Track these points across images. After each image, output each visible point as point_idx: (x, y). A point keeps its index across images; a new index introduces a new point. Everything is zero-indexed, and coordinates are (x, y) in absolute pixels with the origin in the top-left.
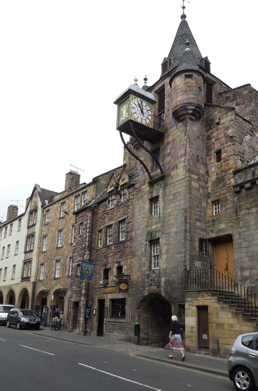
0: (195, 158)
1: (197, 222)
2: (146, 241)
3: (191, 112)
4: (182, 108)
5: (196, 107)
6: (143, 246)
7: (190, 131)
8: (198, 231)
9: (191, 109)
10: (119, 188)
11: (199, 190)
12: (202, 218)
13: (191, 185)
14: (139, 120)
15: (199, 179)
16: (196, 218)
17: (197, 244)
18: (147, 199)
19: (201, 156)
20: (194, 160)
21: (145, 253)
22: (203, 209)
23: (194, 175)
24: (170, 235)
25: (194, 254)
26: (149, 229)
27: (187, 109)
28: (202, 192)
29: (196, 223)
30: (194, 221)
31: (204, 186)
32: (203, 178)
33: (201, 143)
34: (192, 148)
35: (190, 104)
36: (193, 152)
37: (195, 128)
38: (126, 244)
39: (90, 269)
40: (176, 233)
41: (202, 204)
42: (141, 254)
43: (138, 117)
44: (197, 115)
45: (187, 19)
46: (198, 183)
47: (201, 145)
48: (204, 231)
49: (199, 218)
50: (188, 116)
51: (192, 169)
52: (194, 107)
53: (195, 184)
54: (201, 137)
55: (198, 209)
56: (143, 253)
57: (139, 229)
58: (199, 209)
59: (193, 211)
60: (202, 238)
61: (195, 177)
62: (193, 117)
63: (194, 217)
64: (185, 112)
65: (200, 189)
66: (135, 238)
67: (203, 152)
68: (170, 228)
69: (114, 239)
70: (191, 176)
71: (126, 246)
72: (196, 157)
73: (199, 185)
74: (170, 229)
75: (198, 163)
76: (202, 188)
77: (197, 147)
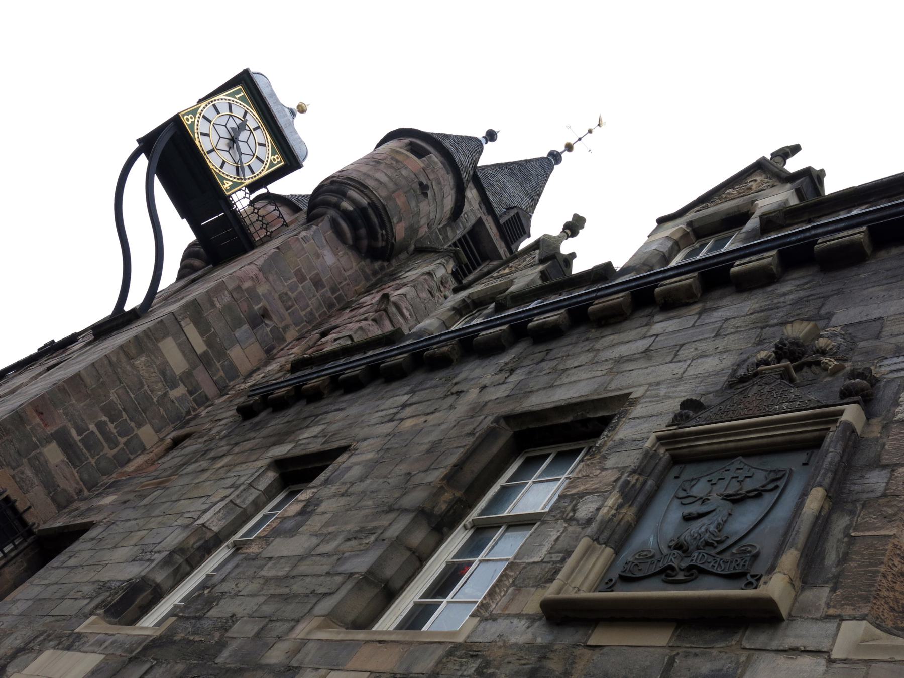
1: (54, 445)
3: (350, 208)
4: (333, 187)
5: (372, 205)
7: (305, 245)
8: (29, 473)
9: (353, 201)
12: (93, 462)
13: (158, 340)
14: (204, 144)
15: (205, 360)
19: (281, 326)
20: (244, 306)
22: (125, 439)
23: (202, 335)
27: (344, 195)
28: (181, 399)
29: (47, 440)
30: (51, 430)
31: (206, 396)
32: (222, 373)
33: (313, 303)
34: (267, 279)
35: (362, 187)
36: (262, 290)
37: (329, 259)
41: (139, 426)
43: (224, 162)
44: (363, 231)
46: (193, 366)
47: (308, 306)
48: (53, 499)
49: (80, 444)
50: (332, 213)
51: (210, 315)
52: (364, 202)
53: (172, 354)
54: (326, 291)
55: (104, 418)
58: (111, 426)
59: (77, 404)
60: (20, 506)
61: (200, 346)
62: (344, 225)
64: (334, 199)
65: (182, 385)
67: (296, 325)
70: (182, 323)
72: (256, 308)
75: (246, 327)
76: (191, 393)
77: (290, 293)
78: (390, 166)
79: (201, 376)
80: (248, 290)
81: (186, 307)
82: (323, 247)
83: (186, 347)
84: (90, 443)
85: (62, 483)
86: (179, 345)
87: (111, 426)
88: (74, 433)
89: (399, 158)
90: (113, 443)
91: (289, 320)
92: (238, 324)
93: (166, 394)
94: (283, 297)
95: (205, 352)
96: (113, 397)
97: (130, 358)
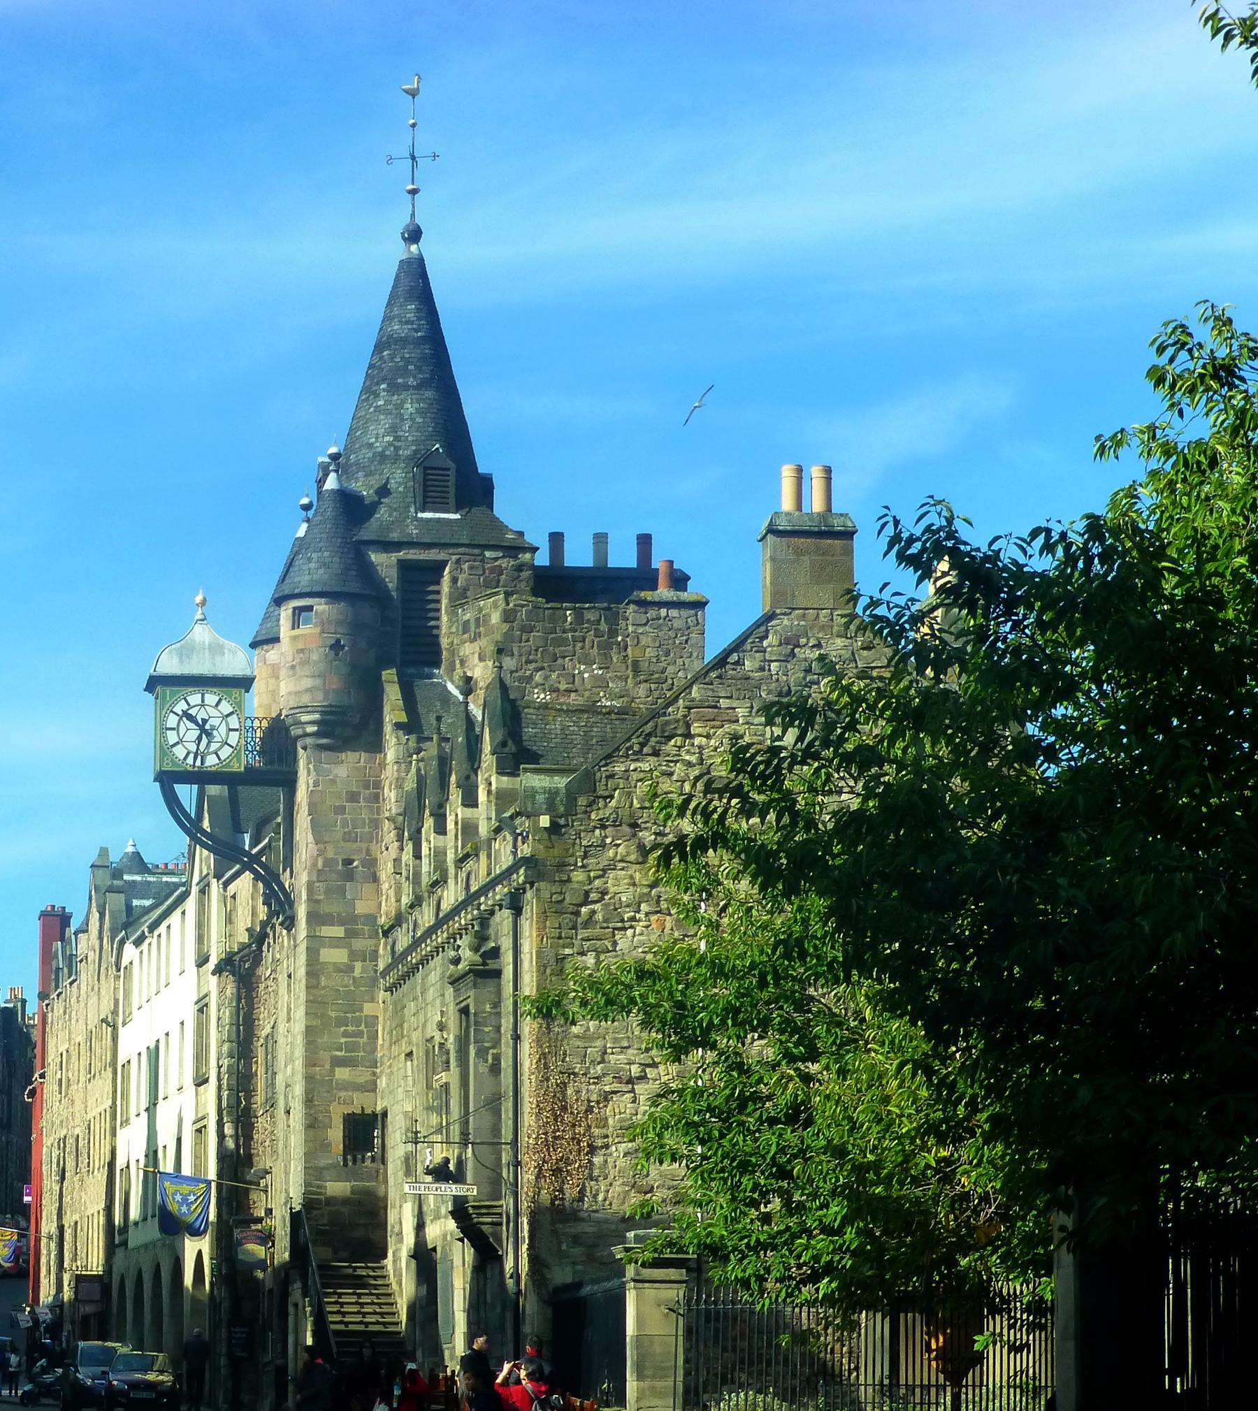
0: (337, 872)
3: (316, 728)
8: (343, 1094)
11: (352, 969)
15: (351, 934)
16: (337, 1057)
17: (336, 1135)
20: (335, 876)
25: (323, 1162)
28: (364, 970)
29: (332, 1071)
30: (328, 1067)
35: (305, 708)
36: (330, 854)
39: (192, 1198)
41: (361, 1010)
45: (426, 247)
46: (349, 946)
51: (326, 908)
52: (317, 716)
53: (334, 956)
58: (350, 1028)
59: (325, 1039)
61: (338, 931)
63: (325, 1056)
64: (300, 732)
72: (340, 867)
73: (353, 956)
76: (364, 961)
78: (302, 663)
79: (359, 944)
80: (324, 866)
81: (308, 922)
82: (330, 771)
83: (335, 943)
84: (351, 1048)
85: (362, 1080)
86: (331, 947)
87: (350, 1028)
88: (338, 1053)
89: (301, 646)
90: (360, 1034)
91: (364, 845)
92: (343, 891)
93: (354, 978)
94: (347, 838)
95: (346, 930)
96: (333, 1014)
97: (316, 987)
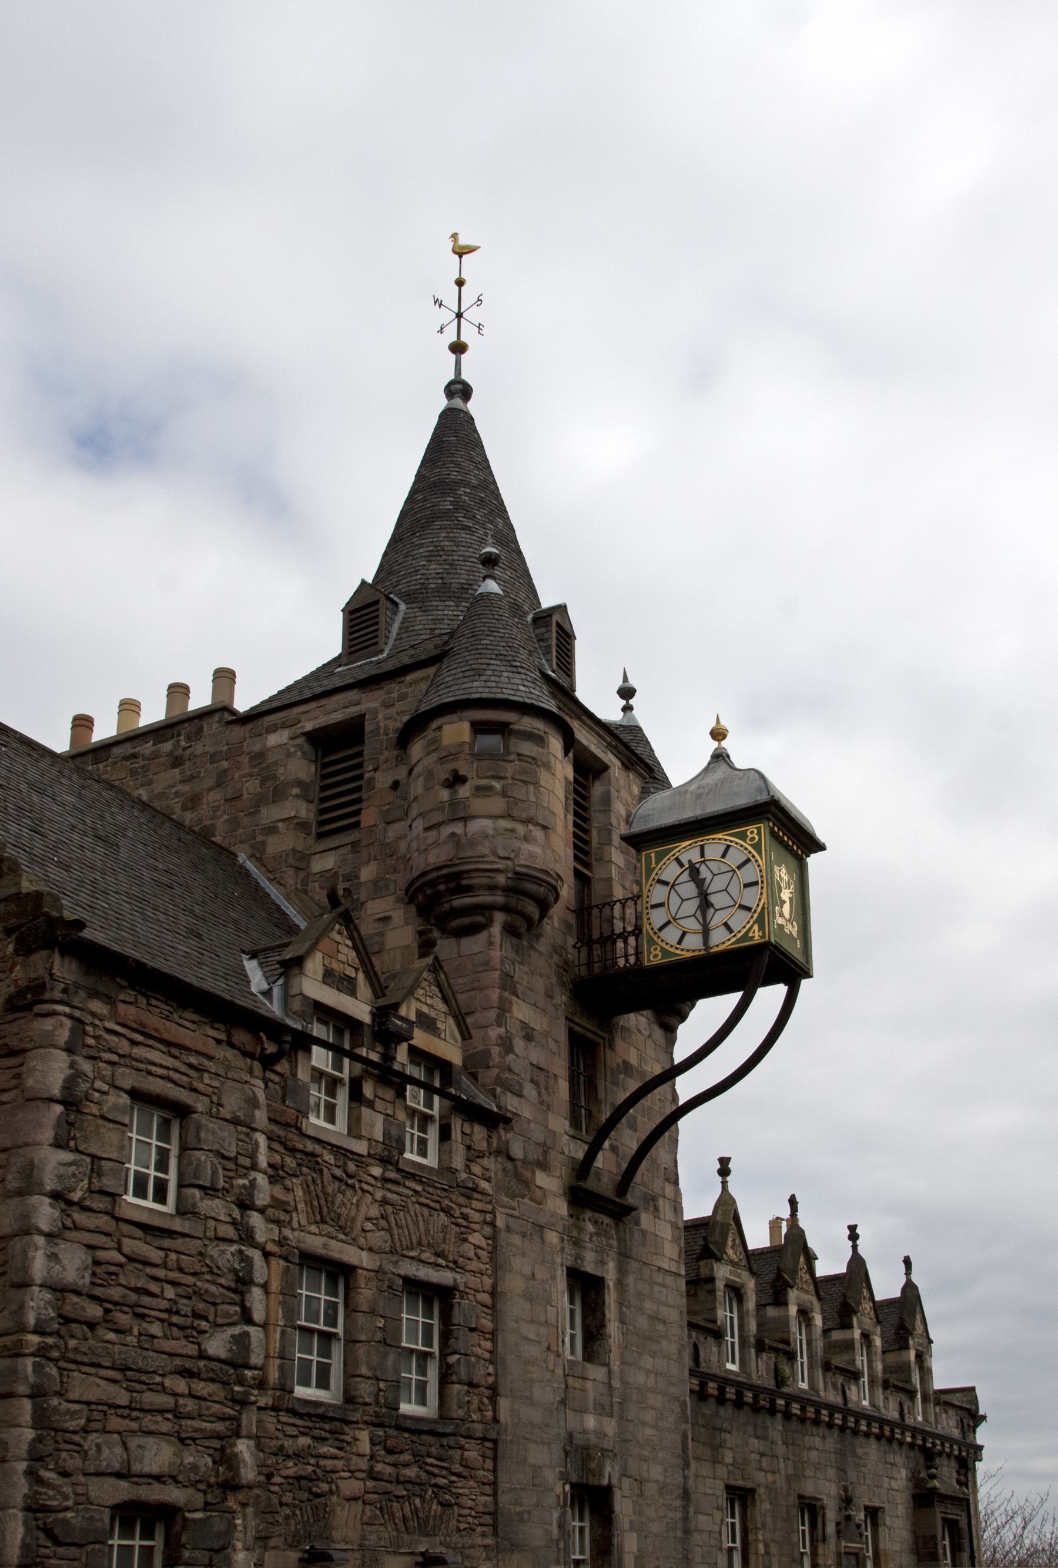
2: (564, 1477)
6: (551, 1500)
10: (402, 1054)
18: (558, 1260)
21: (561, 1545)
24: (651, 1489)
26: (572, 1421)
38: (456, 1454)
40: (662, 1488)
42: (542, 1543)
56: (551, 1540)
57: (530, 1400)
66: (511, 1442)
68: (645, 1460)
69: (382, 1385)
71: (457, 1468)
74: (645, 1466)
